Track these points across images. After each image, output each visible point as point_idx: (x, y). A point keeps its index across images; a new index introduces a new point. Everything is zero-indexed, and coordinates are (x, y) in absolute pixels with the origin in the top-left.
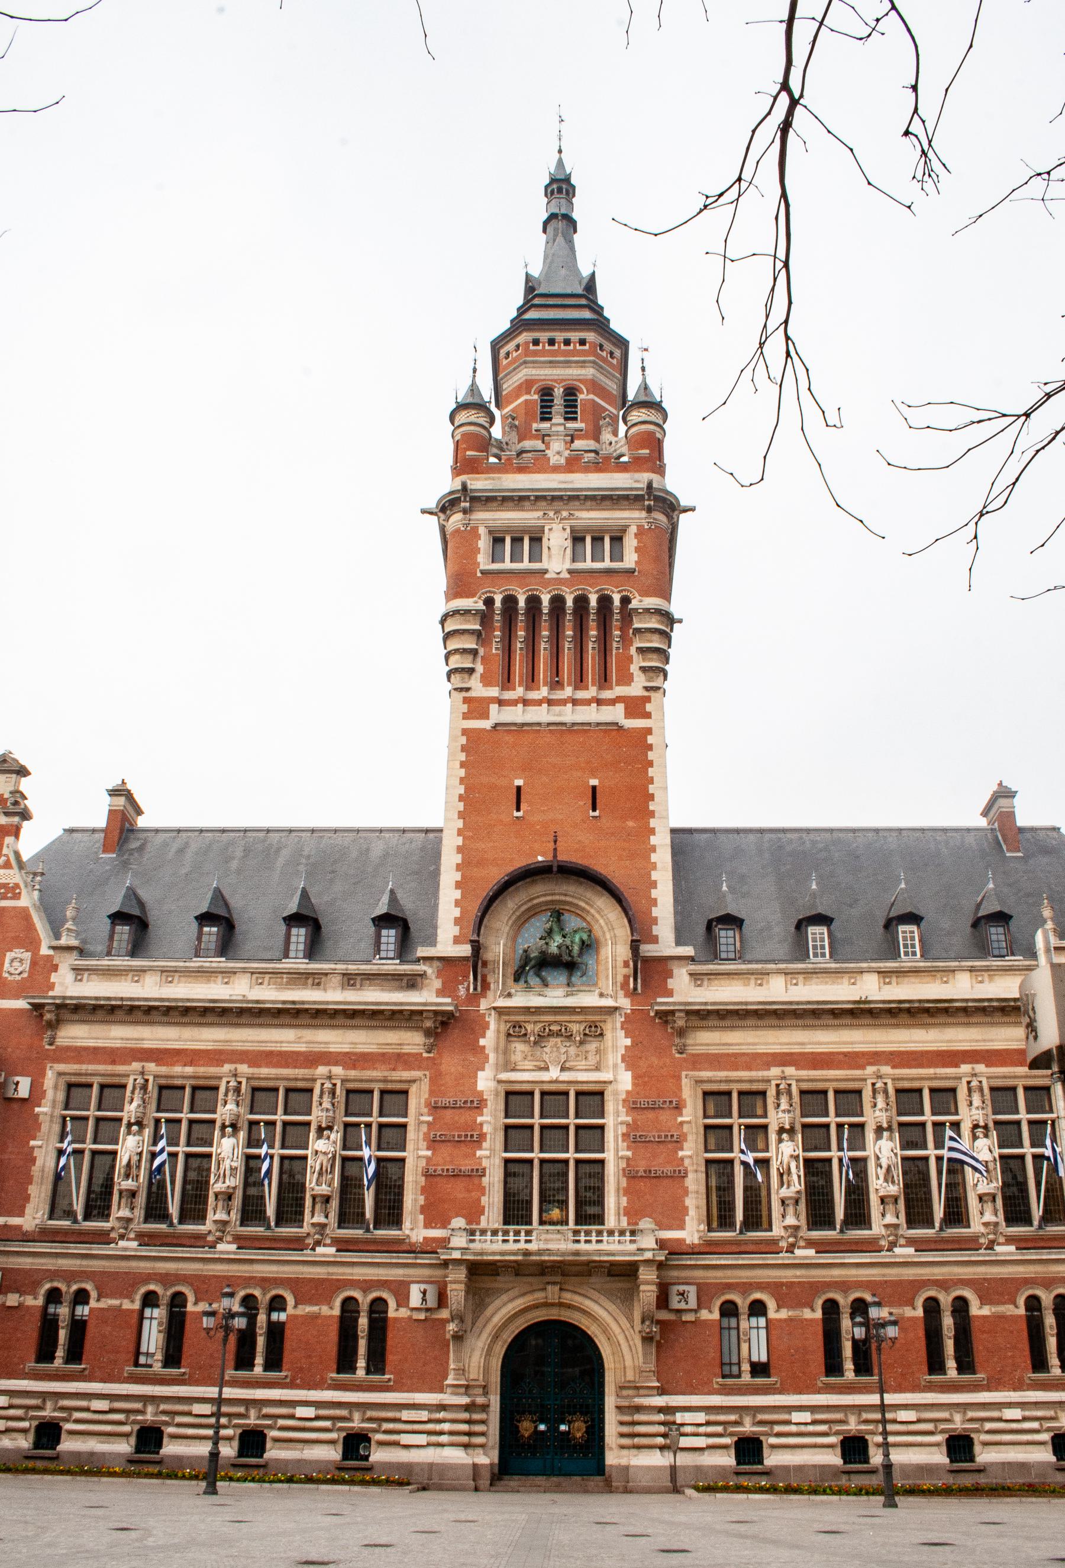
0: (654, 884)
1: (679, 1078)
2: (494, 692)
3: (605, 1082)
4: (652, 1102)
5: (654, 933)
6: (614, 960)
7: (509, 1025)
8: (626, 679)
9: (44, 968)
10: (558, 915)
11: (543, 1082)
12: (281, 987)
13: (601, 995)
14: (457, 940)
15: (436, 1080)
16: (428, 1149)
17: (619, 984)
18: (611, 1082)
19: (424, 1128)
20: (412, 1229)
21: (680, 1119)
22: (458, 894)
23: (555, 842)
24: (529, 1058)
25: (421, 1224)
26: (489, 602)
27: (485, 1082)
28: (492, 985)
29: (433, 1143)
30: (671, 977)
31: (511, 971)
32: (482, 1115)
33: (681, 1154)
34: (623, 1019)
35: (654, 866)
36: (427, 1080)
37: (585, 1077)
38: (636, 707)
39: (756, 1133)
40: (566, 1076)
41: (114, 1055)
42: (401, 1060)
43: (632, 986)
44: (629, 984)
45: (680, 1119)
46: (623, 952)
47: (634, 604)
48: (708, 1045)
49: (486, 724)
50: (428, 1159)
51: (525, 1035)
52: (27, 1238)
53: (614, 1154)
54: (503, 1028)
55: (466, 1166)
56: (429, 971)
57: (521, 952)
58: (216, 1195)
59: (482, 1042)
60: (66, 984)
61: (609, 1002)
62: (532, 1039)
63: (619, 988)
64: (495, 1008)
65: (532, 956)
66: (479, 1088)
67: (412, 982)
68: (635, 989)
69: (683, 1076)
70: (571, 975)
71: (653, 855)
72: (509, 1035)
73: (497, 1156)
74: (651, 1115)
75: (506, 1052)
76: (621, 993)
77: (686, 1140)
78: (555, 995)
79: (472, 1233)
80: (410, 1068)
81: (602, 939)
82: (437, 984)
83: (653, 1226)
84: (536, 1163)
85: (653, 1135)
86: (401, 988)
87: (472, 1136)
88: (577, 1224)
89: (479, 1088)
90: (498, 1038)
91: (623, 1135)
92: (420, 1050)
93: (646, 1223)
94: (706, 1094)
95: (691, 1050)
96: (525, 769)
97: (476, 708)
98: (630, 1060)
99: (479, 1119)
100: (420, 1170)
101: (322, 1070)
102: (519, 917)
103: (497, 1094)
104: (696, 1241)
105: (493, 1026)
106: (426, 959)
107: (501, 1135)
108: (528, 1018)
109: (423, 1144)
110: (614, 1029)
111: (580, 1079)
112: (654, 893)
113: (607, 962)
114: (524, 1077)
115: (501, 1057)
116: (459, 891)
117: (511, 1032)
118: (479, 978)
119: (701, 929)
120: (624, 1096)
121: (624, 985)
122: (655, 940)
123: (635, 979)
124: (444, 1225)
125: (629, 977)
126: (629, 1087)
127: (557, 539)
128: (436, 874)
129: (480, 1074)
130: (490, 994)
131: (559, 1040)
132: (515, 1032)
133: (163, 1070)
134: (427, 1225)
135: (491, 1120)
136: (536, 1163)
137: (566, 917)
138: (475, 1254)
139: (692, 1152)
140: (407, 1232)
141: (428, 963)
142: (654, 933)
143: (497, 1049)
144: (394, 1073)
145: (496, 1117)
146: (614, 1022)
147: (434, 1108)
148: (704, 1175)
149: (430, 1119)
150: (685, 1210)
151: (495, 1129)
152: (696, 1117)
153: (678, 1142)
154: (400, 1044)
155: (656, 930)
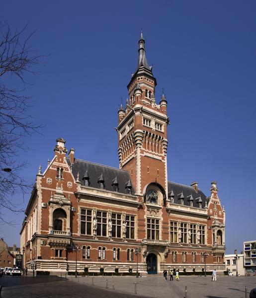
2: (144, 149)
4: (165, 223)
8: (162, 153)
9: (75, 186)
12: (117, 196)
14: (141, 193)
15: (139, 215)
22: (141, 185)
26: (144, 131)
27: (145, 217)
38: (163, 158)
39: (176, 228)
40: (155, 217)
41: (89, 205)
42: (133, 212)
47: (164, 139)
49: (143, 155)
52: (79, 237)
53: (160, 229)
55: (143, 230)
58: (109, 232)
60: (80, 190)
67: (135, 199)
78: (153, 205)
82: (138, 200)
96: (149, 165)
97: (142, 152)
98: (163, 216)
101: (123, 212)
127: (153, 123)
133: (98, 209)
139: (169, 230)
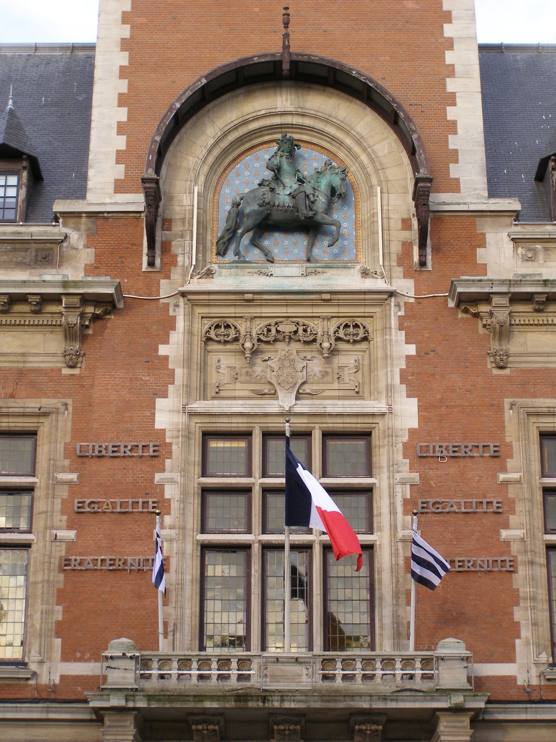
0: (452, 100)
1: (500, 409)
3: (373, 415)
5: (453, 175)
6: (386, 218)
7: (208, 323)
10: (290, 149)
11: (266, 415)
13: (365, 273)
15: (83, 412)
16: (70, 527)
17: (394, 257)
18: (383, 415)
19: (63, 493)
20: (41, 662)
21: (502, 477)
22: (122, 114)
23: (286, 25)
24: (243, 378)
25: (57, 653)
27: (167, 415)
28: (180, 259)
29: (80, 514)
30: (483, 245)
31: (211, 239)
32: (163, 470)
33: (505, 534)
34: (402, 313)
35: (451, 71)
36: (68, 415)
37: (339, 407)
43: (416, 258)
44: (411, 256)
45: (502, 477)
46: (402, 204)
48: (548, 355)
50: (70, 545)
51: (236, 339)
54: (201, 327)
56: (74, 236)
57: (228, 208)
59: (163, 350)
61: (380, 284)
62: (248, 345)
63: (394, 263)
64: (183, 294)
65: (247, 211)
66: (157, 426)
67: (46, 254)
68: (423, 264)
69: (507, 406)
70: (311, 246)
71: (448, 54)
72: (209, 339)
73: (189, 539)
74: (452, 469)
75: (203, 367)
76: (398, 271)
77: (513, 511)
78: (286, 268)
79: (145, 663)
80: (41, 394)
81: (363, 188)
82: (87, 256)
83: (463, 651)
84: (256, 549)
85: (457, 503)
86: (21, 265)
87: (145, 503)
88: (326, 648)
89: (157, 426)
90: (190, 343)
91: (406, 502)
92: (57, 363)
93: (451, 646)
94: (544, 435)
95: (515, 363)
98: (415, 379)
99: (158, 477)
100: (56, 562)
102: (226, 152)
103: (188, 436)
104: (535, 682)
105: (180, 324)
106: (67, 215)
107: (195, 503)
108: (240, 311)
109: (61, 519)
110: (386, 328)
111: (329, 410)
112: (451, 113)
113: (374, 223)
114: (235, 406)
115: (195, 374)
116: (125, 110)
117: (212, 335)
118: (158, 245)
119: (527, 178)
120: (406, 439)
121: (404, 258)
122: (455, 186)
123: (422, 245)
124: (96, 657)
125: (411, 244)
126: (415, 424)
128: (86, 106)
129: (160, 403)
130: (176, 275)
131: (295, 346)
132: (220, 334)
134: (66, 657)
135: (176, 481)
136: (256, 549)
137: (303, 151)
138: (150, 698)
140: (33, 667)
141: (71, 221)
142: (453, 175)
143: (188, 362)
144: (11, 402)
145: (184, 472)
146: (386, 317)
147: (80, 458)
148: (544, 570)
149: (74, 477)
150: (514, 630)
151: (185, 493)
152: (529, 472)
153: (500, 513)
154: (23, 354)
155: (454, 171)
